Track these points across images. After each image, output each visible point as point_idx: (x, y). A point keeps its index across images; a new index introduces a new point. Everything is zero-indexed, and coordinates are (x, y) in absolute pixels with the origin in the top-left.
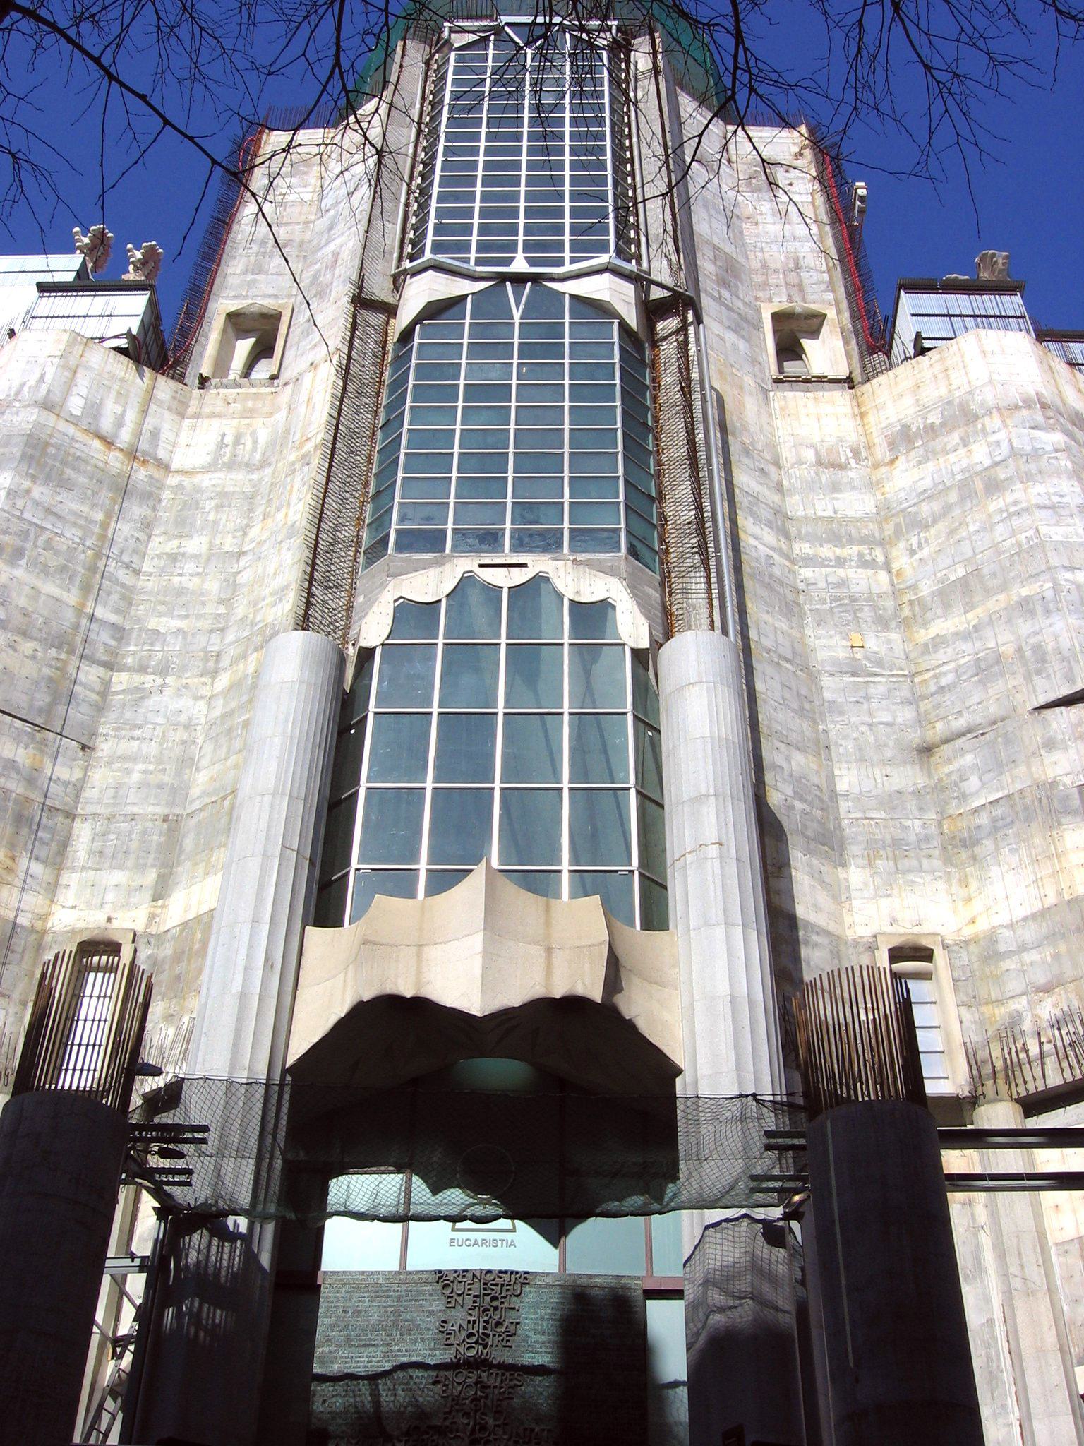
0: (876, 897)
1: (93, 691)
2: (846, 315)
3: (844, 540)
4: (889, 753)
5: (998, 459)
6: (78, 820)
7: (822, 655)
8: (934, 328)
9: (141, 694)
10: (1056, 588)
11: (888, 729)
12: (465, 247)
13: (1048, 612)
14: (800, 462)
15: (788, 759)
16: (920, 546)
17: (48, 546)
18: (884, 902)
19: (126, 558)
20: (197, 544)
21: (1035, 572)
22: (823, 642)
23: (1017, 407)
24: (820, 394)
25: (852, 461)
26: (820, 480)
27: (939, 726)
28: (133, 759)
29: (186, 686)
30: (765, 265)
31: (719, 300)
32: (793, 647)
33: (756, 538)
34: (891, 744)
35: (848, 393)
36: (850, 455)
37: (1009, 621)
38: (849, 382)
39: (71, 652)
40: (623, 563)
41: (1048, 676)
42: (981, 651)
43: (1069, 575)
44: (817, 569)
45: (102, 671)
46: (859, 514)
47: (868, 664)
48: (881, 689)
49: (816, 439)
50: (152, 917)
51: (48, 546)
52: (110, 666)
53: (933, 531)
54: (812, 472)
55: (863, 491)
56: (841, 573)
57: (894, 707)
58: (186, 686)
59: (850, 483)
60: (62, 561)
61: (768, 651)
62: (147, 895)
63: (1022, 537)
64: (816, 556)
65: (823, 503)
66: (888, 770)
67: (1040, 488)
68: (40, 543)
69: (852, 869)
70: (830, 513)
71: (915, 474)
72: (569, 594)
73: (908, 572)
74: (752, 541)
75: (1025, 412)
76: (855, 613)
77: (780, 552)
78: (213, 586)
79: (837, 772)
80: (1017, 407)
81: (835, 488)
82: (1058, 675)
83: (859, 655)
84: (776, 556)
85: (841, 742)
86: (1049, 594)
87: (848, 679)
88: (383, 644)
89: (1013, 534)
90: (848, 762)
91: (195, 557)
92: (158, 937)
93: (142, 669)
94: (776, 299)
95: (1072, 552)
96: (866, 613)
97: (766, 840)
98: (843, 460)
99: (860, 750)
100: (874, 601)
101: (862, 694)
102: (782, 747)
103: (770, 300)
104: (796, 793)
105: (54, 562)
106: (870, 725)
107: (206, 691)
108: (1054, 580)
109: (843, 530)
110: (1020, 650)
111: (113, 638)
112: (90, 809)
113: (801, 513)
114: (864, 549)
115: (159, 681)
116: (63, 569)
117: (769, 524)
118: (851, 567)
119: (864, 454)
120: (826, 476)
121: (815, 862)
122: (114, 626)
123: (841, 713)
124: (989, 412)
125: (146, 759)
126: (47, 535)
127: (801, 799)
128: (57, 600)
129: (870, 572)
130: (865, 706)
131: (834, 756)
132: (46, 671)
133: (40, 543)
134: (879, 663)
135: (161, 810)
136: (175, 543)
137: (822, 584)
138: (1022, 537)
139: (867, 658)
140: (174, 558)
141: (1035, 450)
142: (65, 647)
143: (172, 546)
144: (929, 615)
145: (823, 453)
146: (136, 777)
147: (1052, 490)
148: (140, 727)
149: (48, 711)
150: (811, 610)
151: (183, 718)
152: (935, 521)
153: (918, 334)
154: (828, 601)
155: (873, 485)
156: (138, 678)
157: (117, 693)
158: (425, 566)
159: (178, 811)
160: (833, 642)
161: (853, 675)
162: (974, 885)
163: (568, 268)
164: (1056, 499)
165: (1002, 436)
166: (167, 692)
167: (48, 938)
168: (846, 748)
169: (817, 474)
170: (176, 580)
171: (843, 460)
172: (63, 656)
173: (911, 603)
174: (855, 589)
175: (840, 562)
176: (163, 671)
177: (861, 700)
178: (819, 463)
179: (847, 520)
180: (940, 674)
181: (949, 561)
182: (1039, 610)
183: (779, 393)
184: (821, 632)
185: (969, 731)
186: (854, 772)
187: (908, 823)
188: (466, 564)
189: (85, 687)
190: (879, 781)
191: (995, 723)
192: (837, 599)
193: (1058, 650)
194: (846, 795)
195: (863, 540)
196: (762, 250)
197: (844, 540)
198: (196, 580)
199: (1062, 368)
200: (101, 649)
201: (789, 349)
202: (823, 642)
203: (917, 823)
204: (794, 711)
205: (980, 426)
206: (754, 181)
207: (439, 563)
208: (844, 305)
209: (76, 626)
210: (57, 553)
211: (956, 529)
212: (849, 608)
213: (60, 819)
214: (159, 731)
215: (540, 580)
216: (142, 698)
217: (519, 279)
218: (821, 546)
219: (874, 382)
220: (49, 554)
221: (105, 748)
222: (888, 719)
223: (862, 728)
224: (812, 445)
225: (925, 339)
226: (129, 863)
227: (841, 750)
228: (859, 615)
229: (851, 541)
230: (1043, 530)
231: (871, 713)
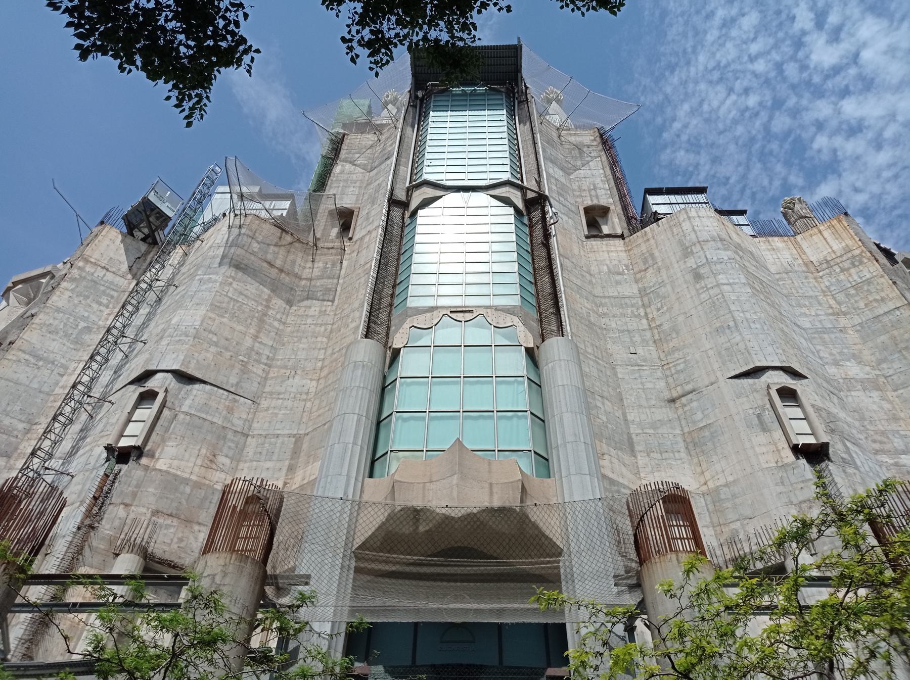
16: (662, 305)
35: (622, 242)
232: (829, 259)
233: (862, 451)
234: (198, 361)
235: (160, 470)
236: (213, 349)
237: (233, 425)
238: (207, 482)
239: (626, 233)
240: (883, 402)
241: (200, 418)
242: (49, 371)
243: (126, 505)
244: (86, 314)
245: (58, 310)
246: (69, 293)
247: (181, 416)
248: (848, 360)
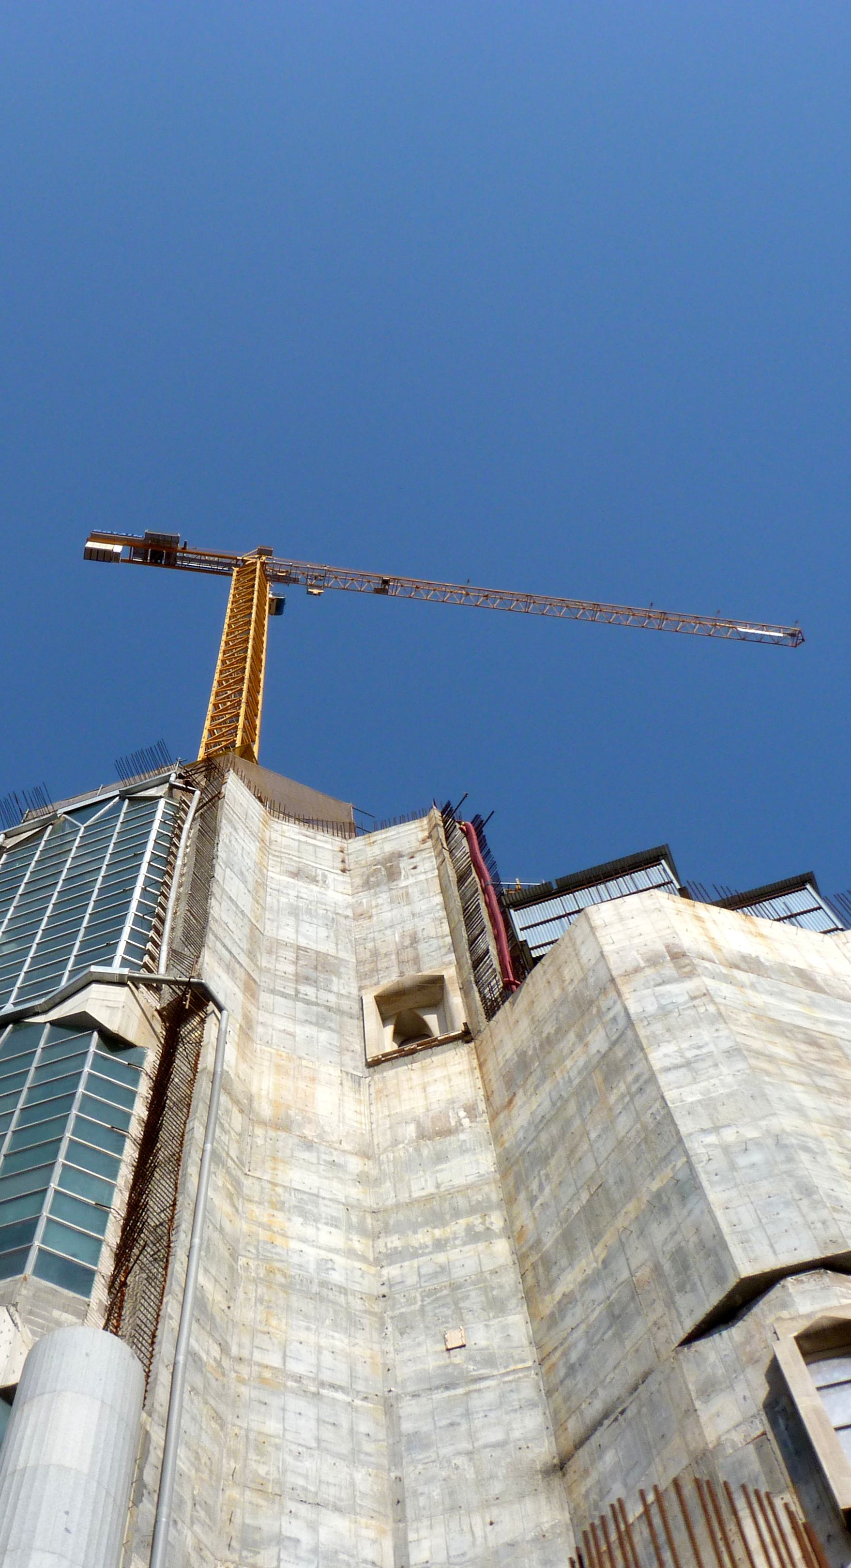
3: (448, 1217)
4: (497, 1488)
5: (614, 1038)
11: (498, 1453)
21: (665, 1152)
24: (428, 1060)
25: (466, 1122)
26: (421, 1155)
34: (501, 1472)
36: (462, 1114)
37: (642, 1233)
42: (612, 1292)
44: (407, 1264)
46: (471, 1179)
47: (471, 1367)
48: (490, 1397)
49: (420, 1111)
53: (553, 1162)
54: (411, 1150)
55: (478, 1150)
56: (441, 1258)
57: (507, 1418)
59: (461, 1147)
65: (423, 1180)
66: (494, 1513)
70: (431, 1189)
71: (535, 1101)
76: (456, 1303)
80: (637, 970)
81: (441, 1158)
82: (706, 1280)
85: (420, 1489)
87: (440, 1396)
90: (431, 1517)
95: (715, 1109)
96: (475, 1299)
98: (453, 1124)
99: (451, 1493)
100: (485, 1280)
101: (460, 1410)
106: (469, 1454)
109: (446, 1205)
110: (657, 1268)
118: (455, 1247)
123: (427, 1446)
130: (464, 1427)
131: (410, 1513)
134: (490, 1360)
137: (412, 1280)
141: (662, 1007)
144: (554, 1271)
150: (392, 1318)
152: (554, 1149)
154: (419, 1298)
160: (421, 1351)
161: (447, 1388)
164: (690, 1054)
168: (429, 1497)
169: (417, 1150)
171: (453, 1124)
175: (440, 1245)
177: (458, 1420)
179: (452, 1193)
180: (569, 1348)
181: (571, 1190)
184: (407, 1341)
185: (606, 1416)
186: (440, 1530)
190: (479, 1533)
191: (635, 1388)
193: (702, 1245)
195: (473, 1210)
196: (374, 940)
197: (448, 1217)
202: (407, 1354)
205: (594, 1011)
206: (372, 879)
211: (577, 1146)
212: (449, 1300)
218: (415, 1232)
223: (459, 1461)
225: (533, 949)
227: (422, 1501)
228: (462, 1305)
229: (457, 1214)
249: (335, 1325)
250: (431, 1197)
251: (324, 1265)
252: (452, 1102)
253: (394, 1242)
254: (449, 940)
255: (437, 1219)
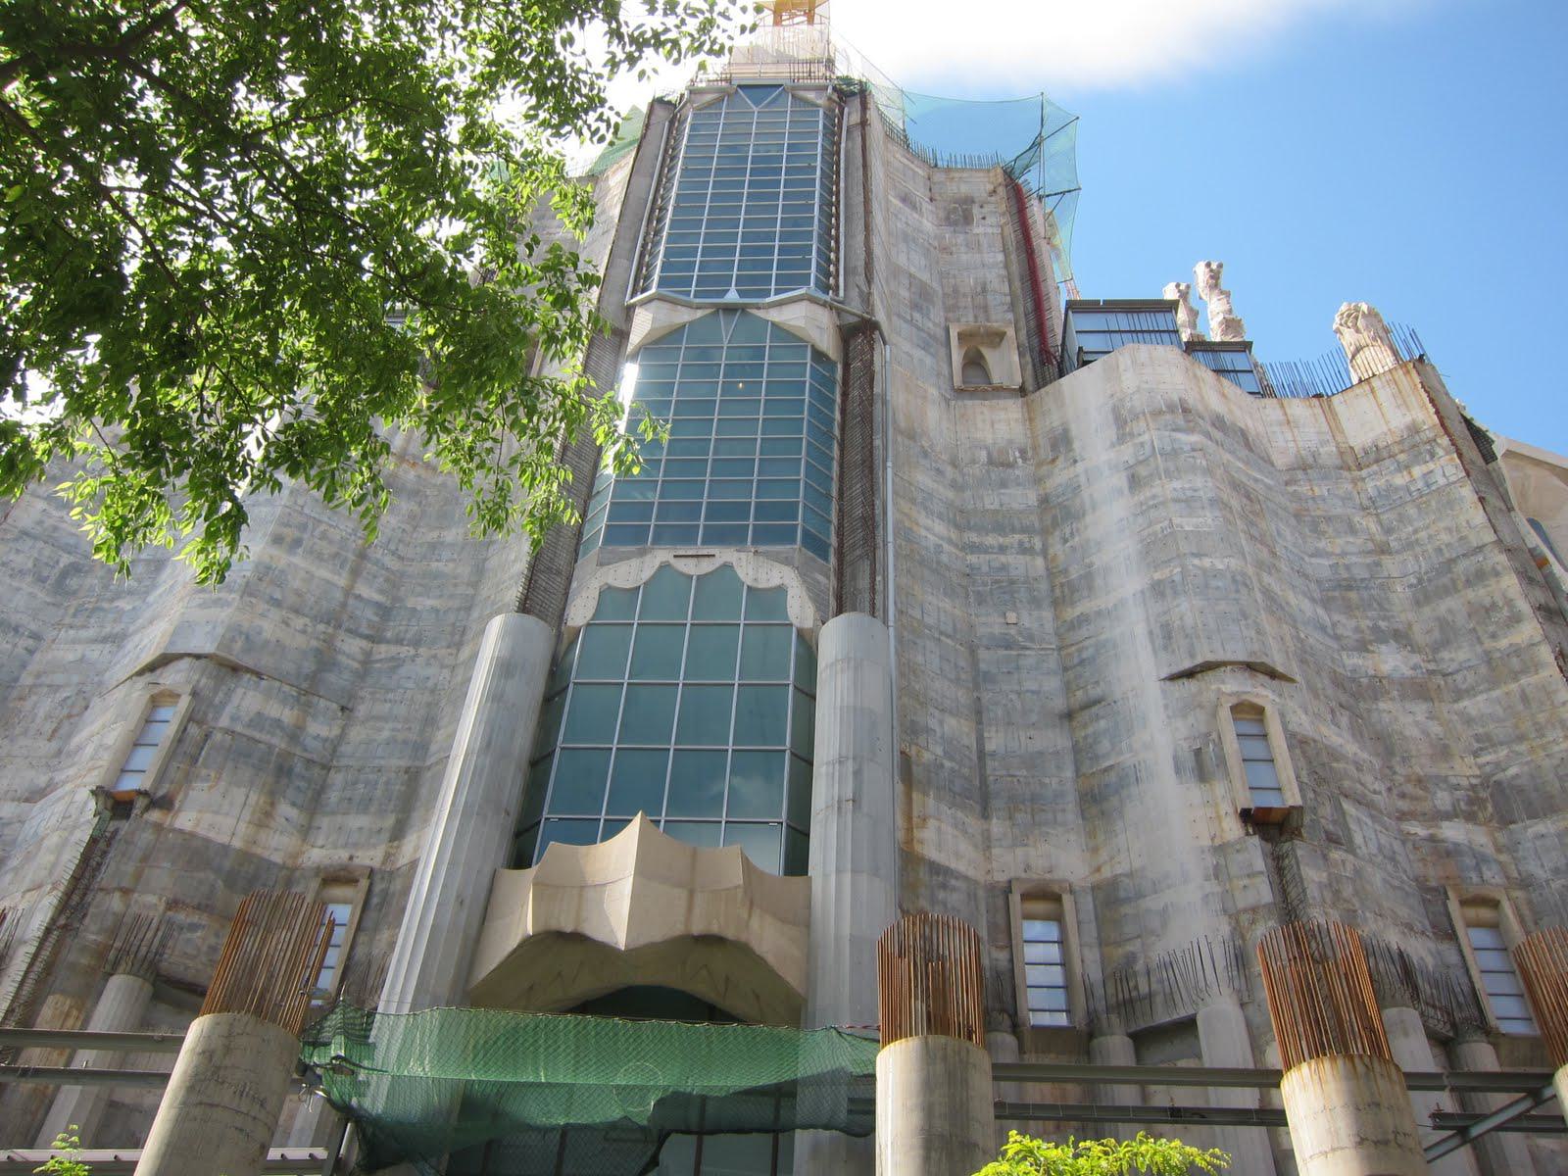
0: (1014, 846)
1: (354, 659)
2: (1024, 332)
4: (1034, 718)
6: (332, 771)
7: (981, 631)
8: (1090, 343)
9: (396, 663)
10: (1184, 573)
12: (688, 282)
13: (1176, 593)
14: (974, 462)
15: (941, 723)
16: (1072, 534)
17: (324, 536)
18: (1020, 851)
19: (392, 547)
20: (451, 535)
22: (983, 619)
23: (1160, 412)
25: (1020, 461)
27: (1079, 693)
28: (384, 719)
29: (435, 657)
30: (956, 291)
31: (911, 322)
32: (954, 625)
33: (927, 529)
35: (1020, 400)
36: (1017, 454)
38: (1022, 391)
39: (339, 626)
40: (796, 555)
41: (1173, 651)
43: (1196, 561)
45: (364, 644)
50: (388, 856)
51: (324, 536)
52: (373, 639)
56: (1003, 559)
58: (435, 657)
60: (334, 549)
61: (930, 628)
62: (385, 836)
63: (1158, 527)
64: (981, 544)
66: (1032, 733)
67: (1177, 484)
68: (317, 533)
69: (995, 821)
70: (996, 506)
72: (748, 581)
73: (1061, 558)
74: (923, 532)
75: (1168, 417)
77: (950, 541)
78: (464, 571)
79: (986, 735)
81: (1003, 484)
83: (1013, 631)
84: (946, 546)
86: (1177, 578)
87: (1002, 652)
88: (588, 625)
89: (1150, 525)
91: (452, 545)
92: (391, 873)
93: (399, 641)
94: (963, 320)
97: (915, 795)
102: (937, 713)
103: (958, 320)
104: (945, 753)
105: (328, 549)
106: (1019, 694)
107: (450, 661)
108: (1183, 566)
111: (377, 614)
112: (344, 762)
113: (970, 507)
114: (1025, 538)
115: (412, 652)
116: (336, 555)
117: (940, 517)
119: (1030, 454)
120: (996, 473)
121: (959, 814)
122: (378, 605)
124: (1136, 417)
125: (396, 719)
126: (323, 527)
127: (951, 759)
128: (328, 582)
129: (1028, 558)
130: (1016, 676)
131: (985, 720)
132: (314, 643)
133: (316, 533)
134: (1031, 638)
135: (404, 763)
136: (435, 534)
138: (1158, 527)
139: (1020, 633)
140: (434, 546)
142: (333, 623)
143: (432, 536)
144: (1076, 596)
145: (995, 454)
146: (386, 734)
147: (1187, 486)
148: (392, 690)
149: (314, 678)
151: (430, 684)
153: (1080, 349)
155: (1038, 481)
156: (394, 649)
157: (377, 661)
158: (627, 557)
159: (417, 763)
162: (1101, 837)
163: (773, 298)
165: (1146, 437)
166: (418, 660)
167: (298, 874)
169: (988, 471)
170: (434, 565)
172: (330, 630)
173: (1062, 585)
174: (1013, 573)
175: (1002, 549)
176: (416, 643)
178: (991, 462)
182: (1168, 592)
183: (960, 403)
187: (1047, 781)
188: (662, 555)
189: (348, 656)
192: (996, 582)
193: (1183, 628)
194: (993, 754)
195: (1024, 530)
198: (451, 565)
199: (1209, 376)
200: (364, 624)
201: (974, 362)
202: (983, 619)
203: (1055, 781)
204: (951, 681)
207: (642, 553)
208: (1022, 323)
209: (344, 605)
210: (331, 542)
213: (316, 771)
214: (409, 694)
215: (727, 567)
216: (398, 667)
217: (730, 309)
219: (1043, 390)
220: (324, 543)
221: (362, 710)
222: (1034, 687)
224: (987, 448)
226: (372, 809)
227: (992, 715)
229: (1013, 531)
230: (1177, 521)
231: (1019, 683)
232: (1381, 444)
233: (1372, 817)
234: (247, 637)
235: (181, 831)
236: (276, 614)
237: (306, 750)
238: (259, 851)
239: (1030, 386)
240: (1430, 723)
241: (250, 739)
242: (9, 646)
243: (126, 892)
244: (72, 541)
245: (25, 533)
246: (41, 505)
247: (218, 736)
248: (1385, 641)
249: (945, 594)
250: (996, 511)
251: (939, 548)
252: (1010, 442)
253: (974, 537)
254: (1008, 299)
255: (1000, 529)
